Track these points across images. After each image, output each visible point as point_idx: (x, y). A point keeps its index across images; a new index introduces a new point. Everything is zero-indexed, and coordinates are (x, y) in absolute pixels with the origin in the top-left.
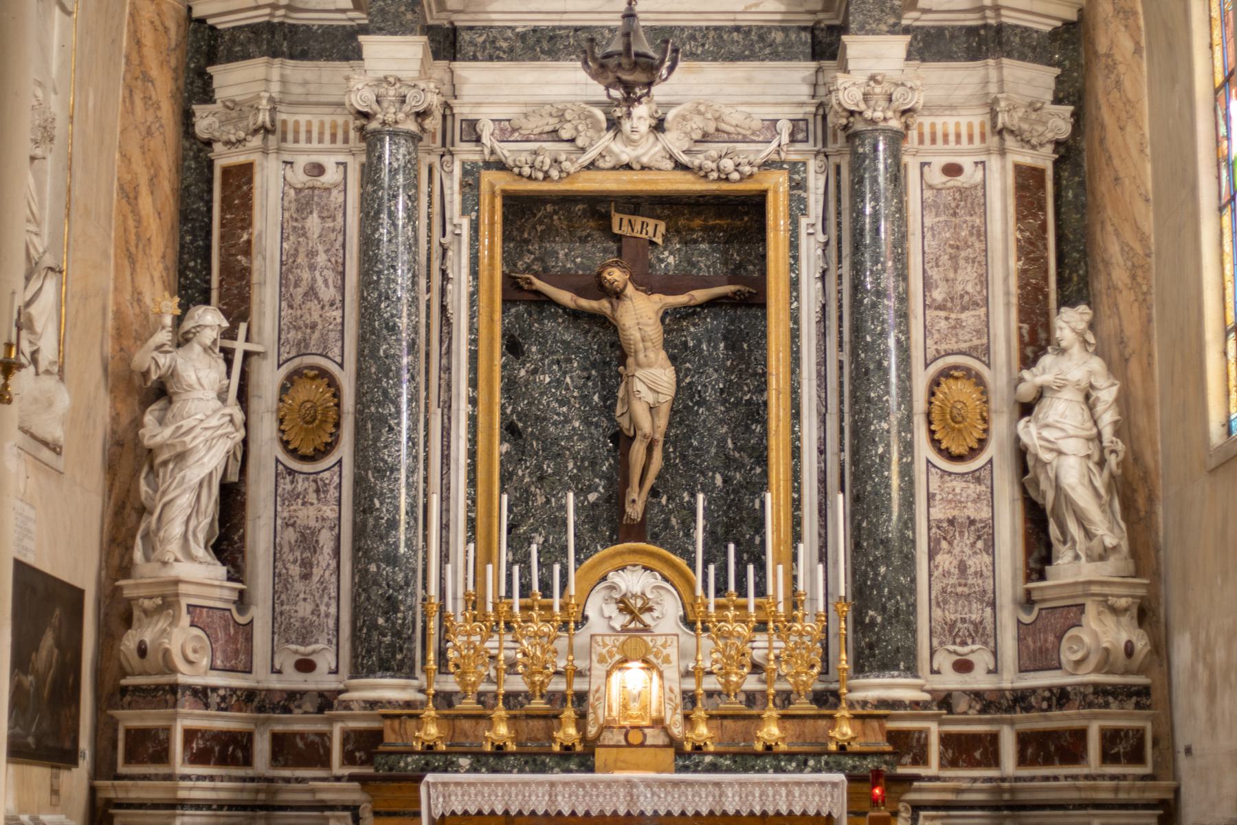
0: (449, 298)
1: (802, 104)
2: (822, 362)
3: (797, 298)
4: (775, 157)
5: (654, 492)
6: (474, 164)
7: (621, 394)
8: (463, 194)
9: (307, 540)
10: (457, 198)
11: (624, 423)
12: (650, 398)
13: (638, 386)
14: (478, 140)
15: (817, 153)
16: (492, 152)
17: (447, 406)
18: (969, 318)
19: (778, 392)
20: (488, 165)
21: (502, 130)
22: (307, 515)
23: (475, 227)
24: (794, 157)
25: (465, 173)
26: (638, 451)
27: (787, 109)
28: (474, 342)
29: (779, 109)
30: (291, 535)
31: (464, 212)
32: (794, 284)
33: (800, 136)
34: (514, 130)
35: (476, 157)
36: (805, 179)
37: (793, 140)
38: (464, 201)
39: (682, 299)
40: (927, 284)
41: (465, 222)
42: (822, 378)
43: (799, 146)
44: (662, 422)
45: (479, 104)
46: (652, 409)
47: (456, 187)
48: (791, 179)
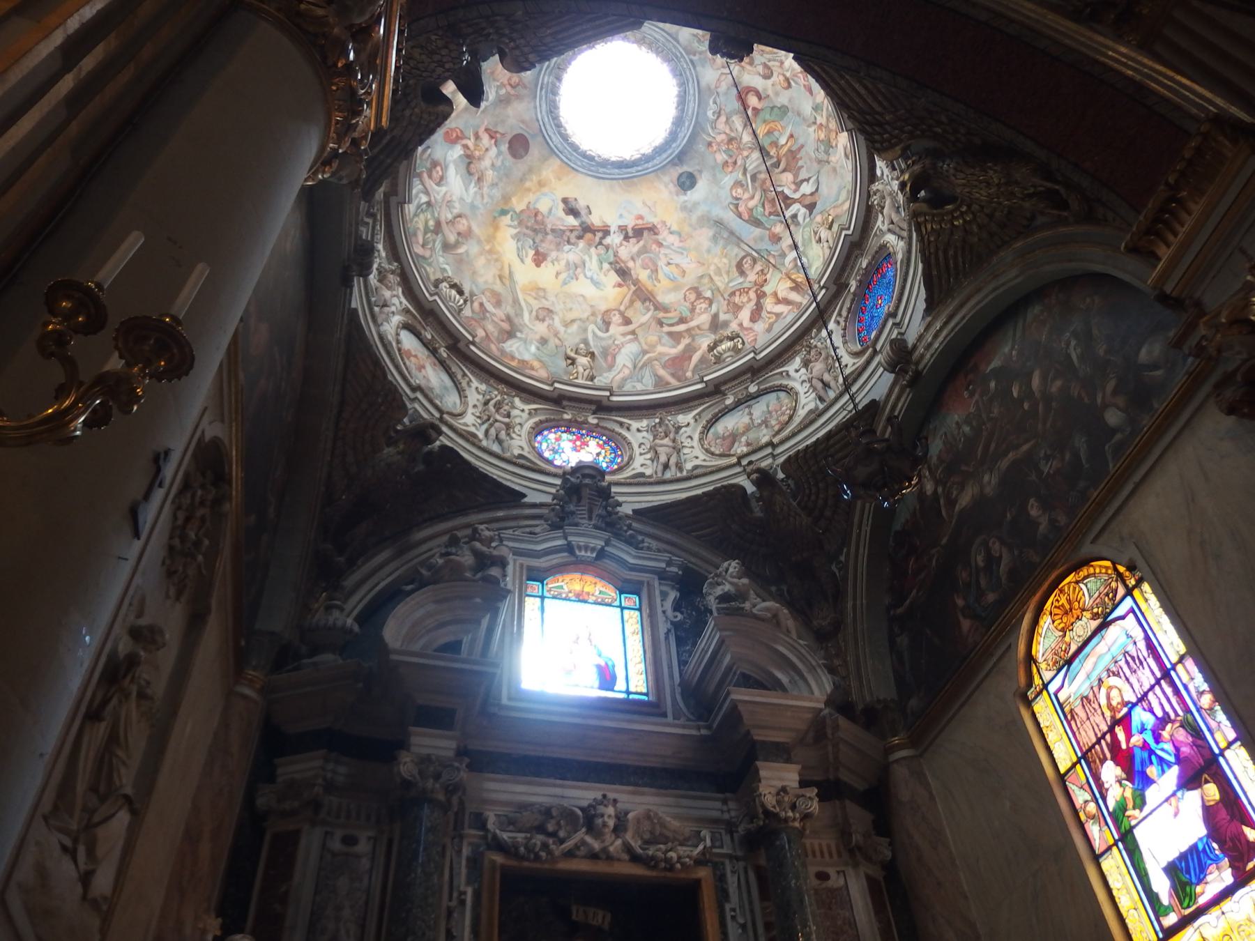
23: (477, 895)
41: (470, 891)
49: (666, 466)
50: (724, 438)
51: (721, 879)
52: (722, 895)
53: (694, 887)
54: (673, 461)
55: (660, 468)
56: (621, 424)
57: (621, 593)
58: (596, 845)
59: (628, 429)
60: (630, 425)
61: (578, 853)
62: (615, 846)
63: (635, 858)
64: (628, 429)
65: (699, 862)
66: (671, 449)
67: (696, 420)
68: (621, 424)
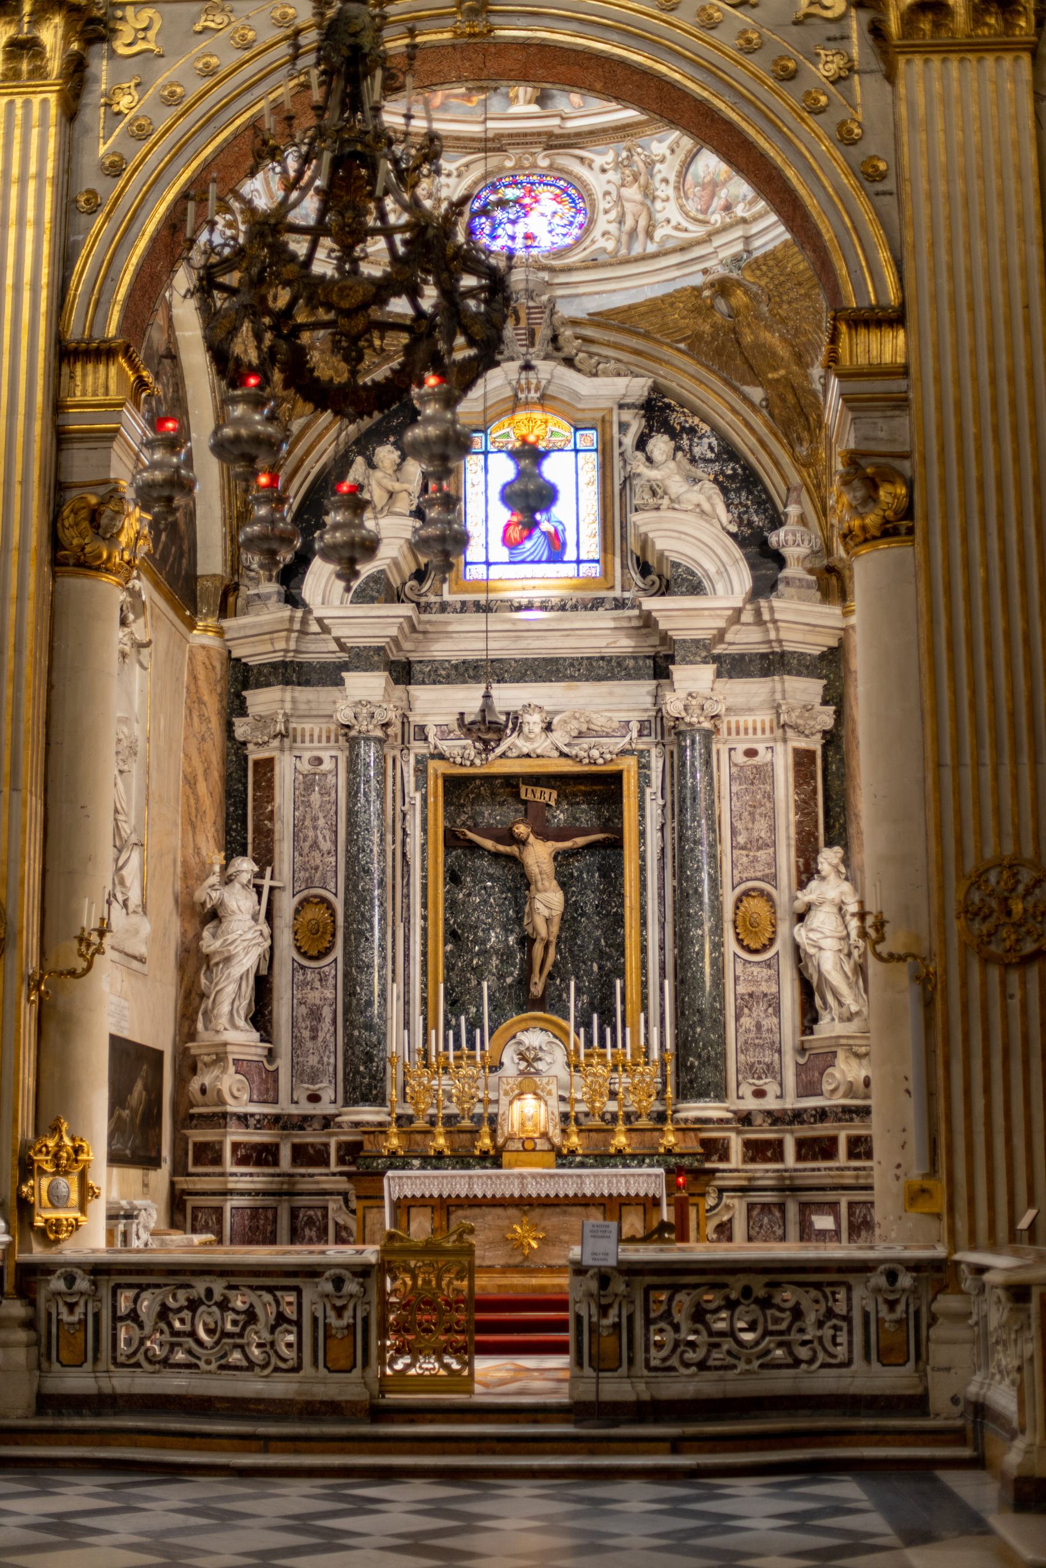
0: (408, 848)
1: (646, 710)
2: (662, 887)
3: (644, 844)
4: (628, 747)
5: (551, 976)
6: (424, 755)
7: (527, 909)
8: (416, 776)
9: (315, 1014)
10: (412, 779)
11: (529, 929)
12: (546, 913)
13: (538, 905)
14: (426, 739)
15: (657, 744)
16: (436, 747)
17: (407, 921)
18: (762, 855)
19: (631, 909)
20: (433, 756)
21: (442, 732)
22: (314, 997)
23: (425, 799)
24: (641, 747)
25: (417, 762)
26: (538, 949)
27: (636, 714)
28: (425, 877)
29: (631, 714)
30: (303, 1010)
31: (417, 789)
32: (642, 834)
33: (646, 732)
34: (450, 732)
35: (425, 751)
36: (649, 762)
37: (640, 734)
38: (417, 782)
39: (567, 844)
40: (734, 832)
41: (418, 796)
42: (662, 898)
43: (645, 739)
44: (555, 929)
45: (426, 715)
46: (548, 920)
47: (412, 772)
48: (639, 762)
49: (633, 234)
50: (703, 186)
51: (644, 766)
52: (644, 781)
53: (616, 778)
54: (642, 223)
55: (624, 238)
56: (582, 159)
57: (577, 429)
58: (526, 747)
59: (590, 167)
60: (592, 161)
61: (509, 754)
62: (541, 744)
63: (563, 755)
64: (590, 167)
65: (623, 752)
66: (640, 207)
67: (673, 151)
68: (582, 159)
